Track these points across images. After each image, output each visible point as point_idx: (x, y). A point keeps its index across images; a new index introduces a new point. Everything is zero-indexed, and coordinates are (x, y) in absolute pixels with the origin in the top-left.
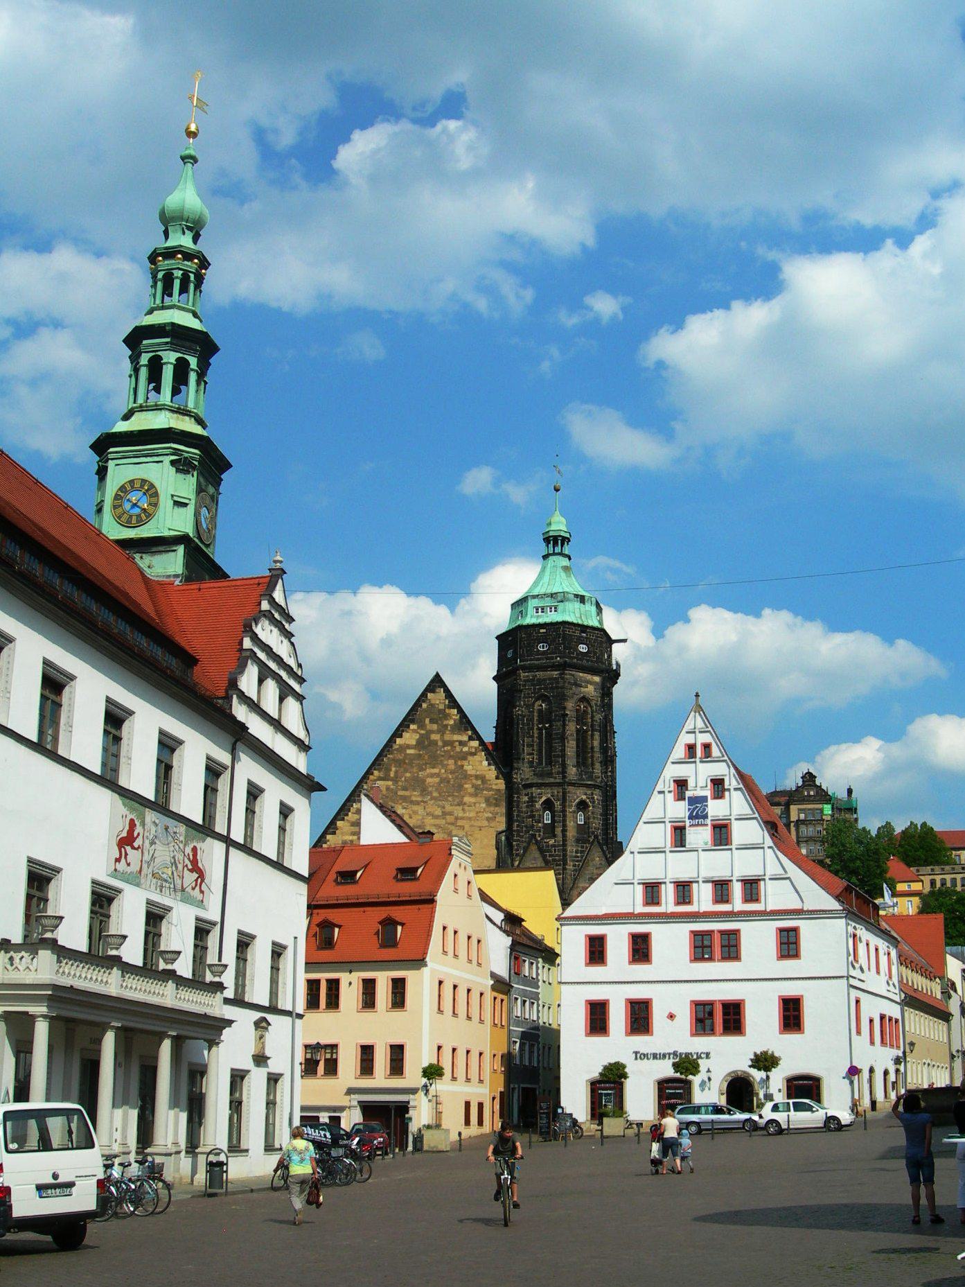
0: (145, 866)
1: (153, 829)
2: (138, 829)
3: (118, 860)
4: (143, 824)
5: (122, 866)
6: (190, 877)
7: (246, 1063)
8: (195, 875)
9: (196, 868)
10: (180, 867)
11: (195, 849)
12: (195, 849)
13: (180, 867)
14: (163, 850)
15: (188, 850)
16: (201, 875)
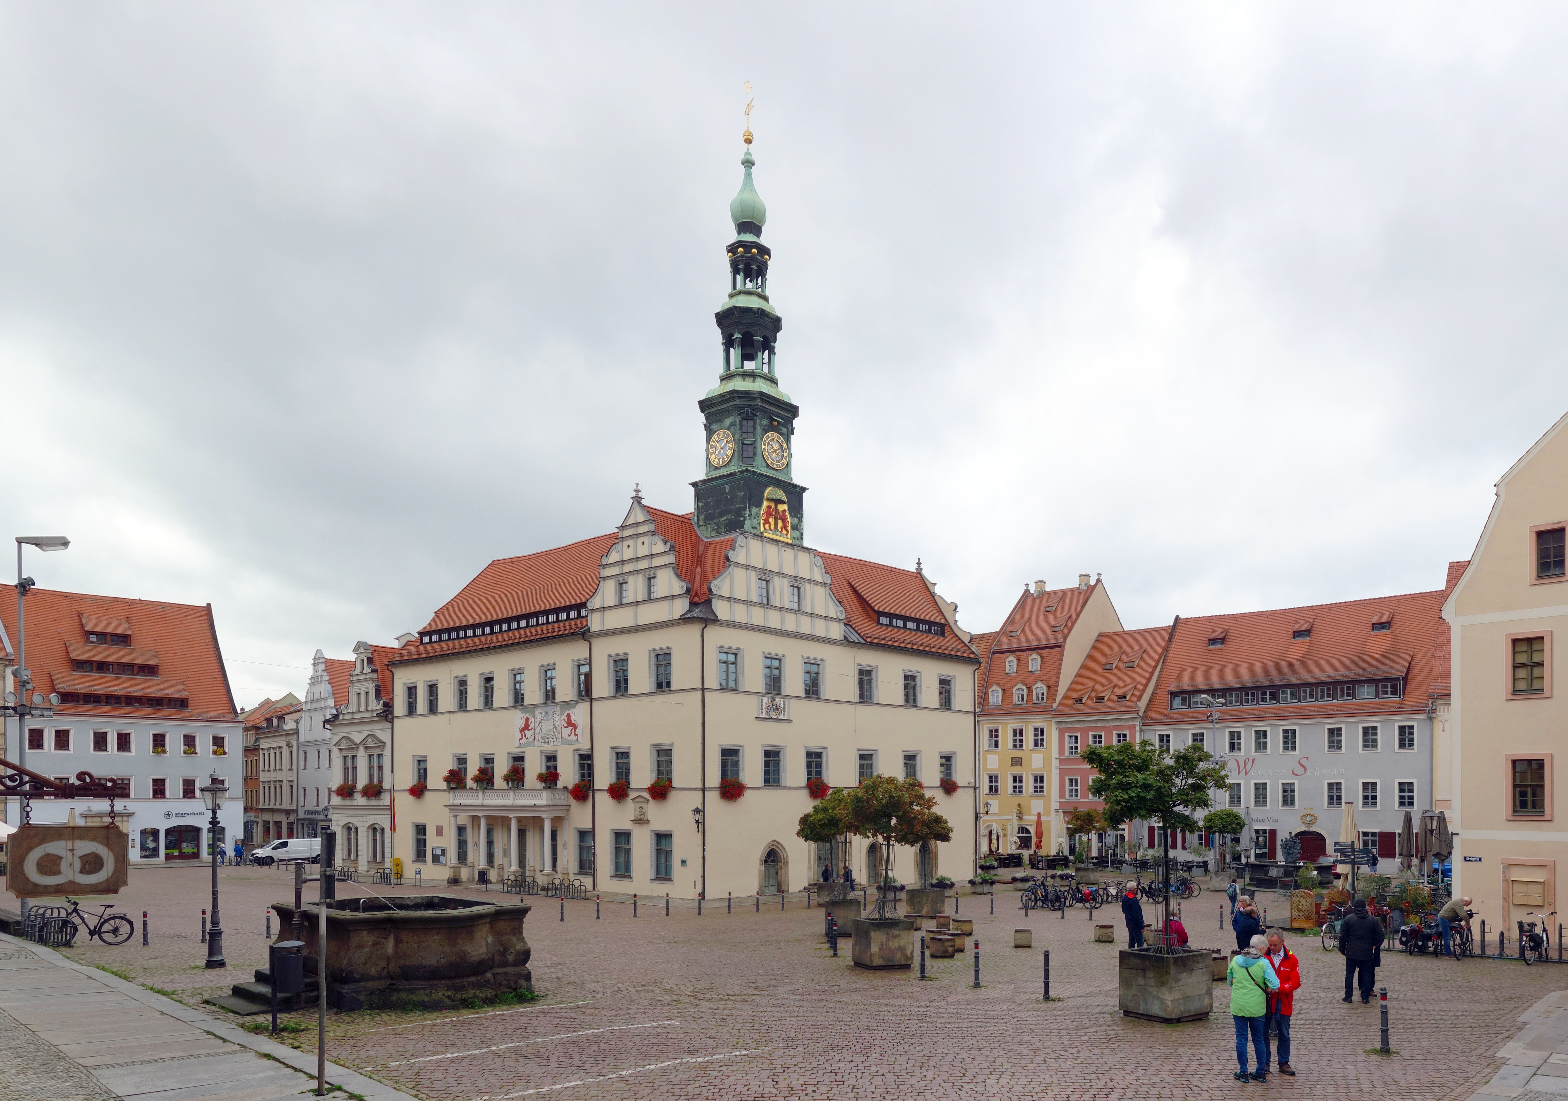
0: (536, 736)
1: (540, 716)
2: (531, 720)
3: (521, 739)
4: (534, 717)
5: (523, 741)
6: (567, 731)
7: (625, 825)
8: (570, 728)
9: (570, 724)
10: (559, 728)
11: (569, 716)
12: (569, 716)
13: (559, 728)
14: (548, 723)
15: (564, 717)
16: (574, 726)
